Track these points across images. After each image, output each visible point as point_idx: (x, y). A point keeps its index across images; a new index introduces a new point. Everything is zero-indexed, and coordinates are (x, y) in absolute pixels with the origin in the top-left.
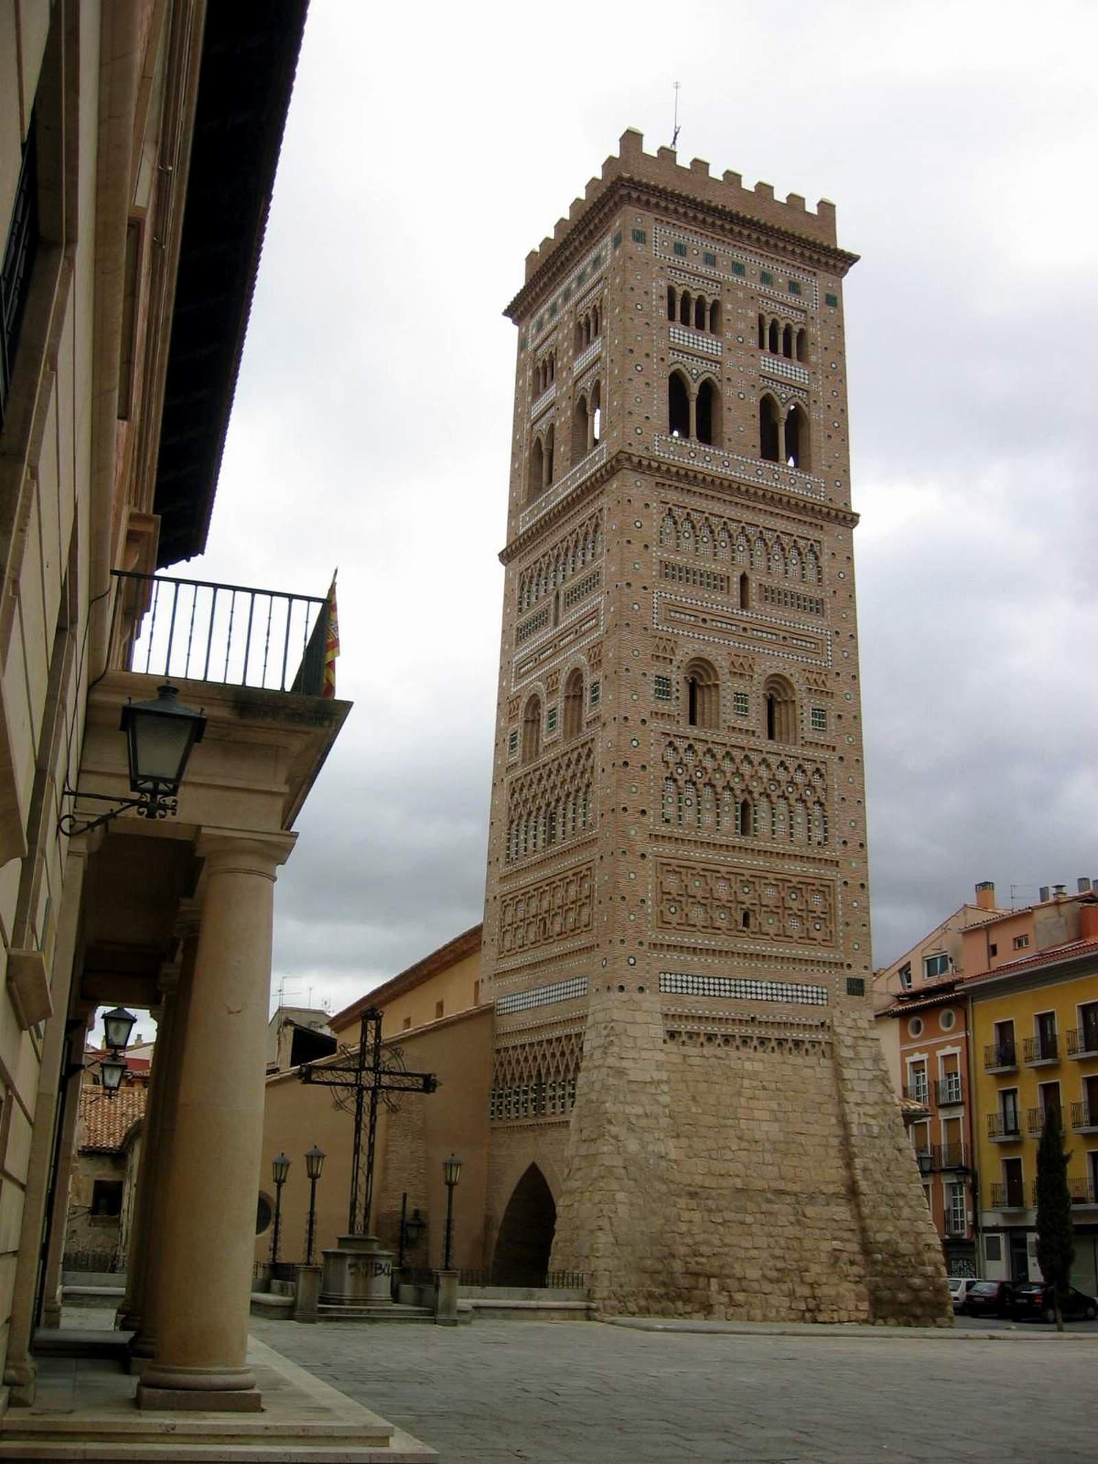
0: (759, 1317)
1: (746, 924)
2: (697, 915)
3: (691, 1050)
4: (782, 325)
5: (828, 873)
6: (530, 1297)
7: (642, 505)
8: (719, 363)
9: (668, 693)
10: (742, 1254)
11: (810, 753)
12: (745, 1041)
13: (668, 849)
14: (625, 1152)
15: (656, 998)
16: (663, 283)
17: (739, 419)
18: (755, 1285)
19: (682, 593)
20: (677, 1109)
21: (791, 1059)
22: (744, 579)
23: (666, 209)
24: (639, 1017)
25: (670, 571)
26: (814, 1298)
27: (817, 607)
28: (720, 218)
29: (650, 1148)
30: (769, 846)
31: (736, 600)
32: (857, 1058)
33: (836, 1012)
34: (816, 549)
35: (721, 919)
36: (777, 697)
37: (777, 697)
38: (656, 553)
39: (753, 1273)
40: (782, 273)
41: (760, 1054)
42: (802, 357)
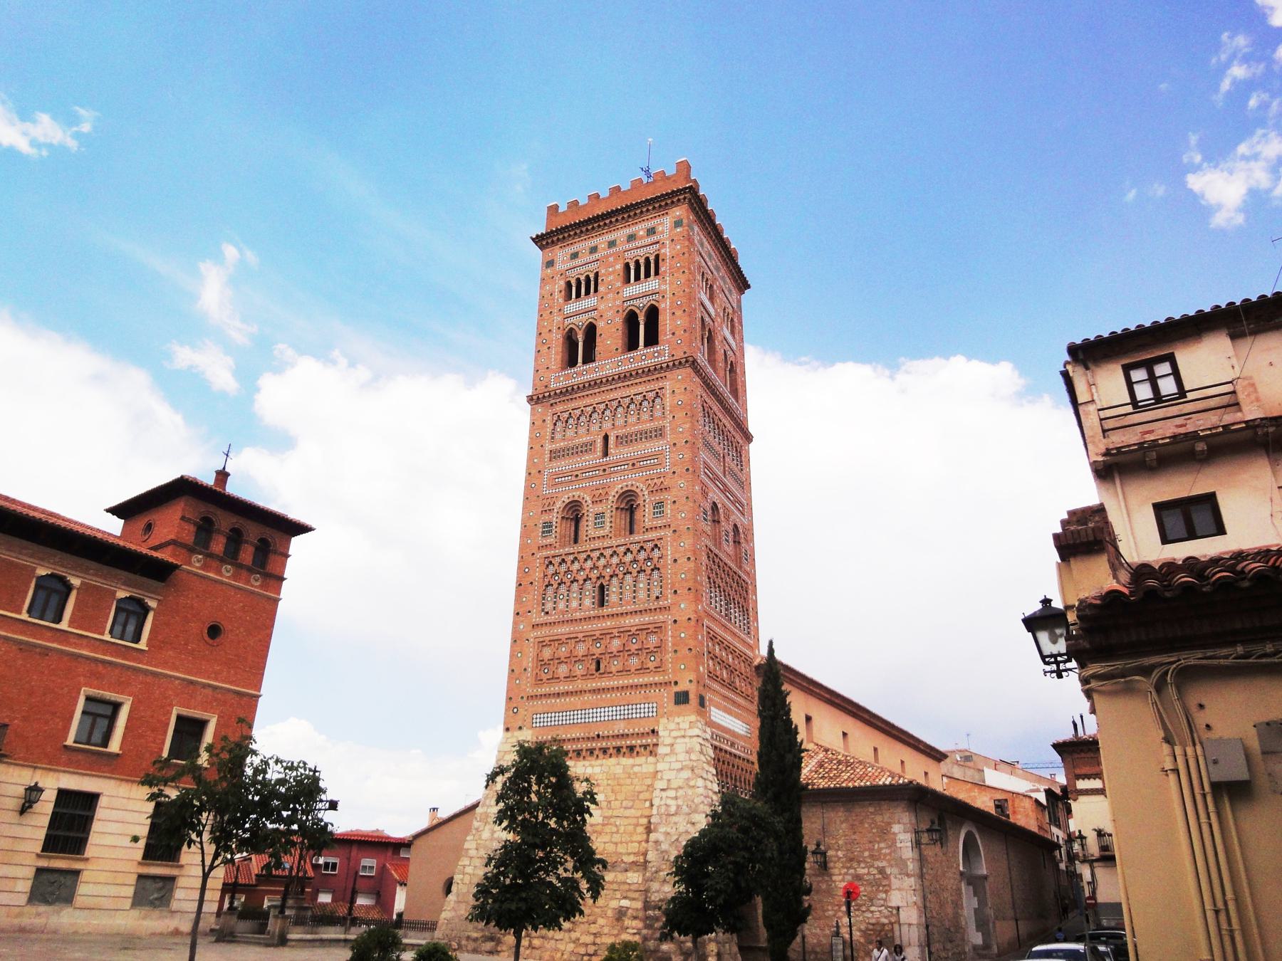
1: (598, 669)
2: (563, 670)
4: (642, 261)
5: (660, 617)
12: (591, 751)
13: (545, 631)
15: (530, 732)
16: (562, 283)
17: (610, 335)
19: (563, 465)
25: (555, 455)
26: (594, 944)
27: (659, 433)
29: (496, 835)
31: (599, 454)
32: (672, 752)
33: (663, 721)
35: (579, 669)
37: (629, 504)
38: (548, 447)
40: (640, 228)
41: (599, 762)
42: (657, 273)
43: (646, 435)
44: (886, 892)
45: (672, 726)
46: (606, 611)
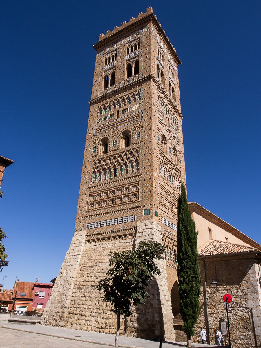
0: (86, 329)
3: (93, 244)
5: (138, 179)
6: (31, 319)
7: (94, 110)
8: (116, 66)
9: (96, 151)
10: (86, 307)
11: (134, 147)
14: (62, 276)
15: (85, 231)
18: (87, 318)
20: (82, 262)
21: (122, 241)
22: (118, 111)
23: (104, 44)
24: (79, 238)
27: (139, 106)
28: (116, 35)
29: (68, 275)
30: (120, 178)
34: (140, 91)
36: (127, 137)
37: (127, 137)
39: (88, 313)
41: (112, 242)
43: (133, 108)
44: (246, 301)
45: (142, 224)
46: (116, 179)
